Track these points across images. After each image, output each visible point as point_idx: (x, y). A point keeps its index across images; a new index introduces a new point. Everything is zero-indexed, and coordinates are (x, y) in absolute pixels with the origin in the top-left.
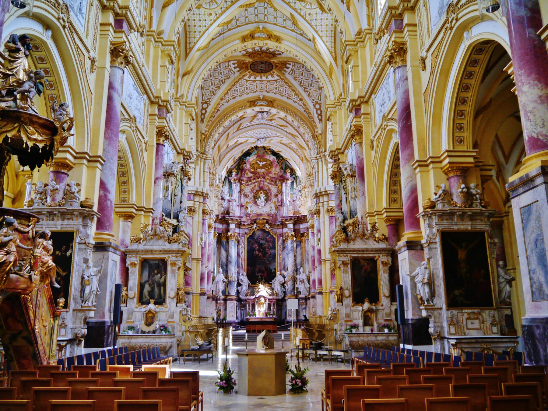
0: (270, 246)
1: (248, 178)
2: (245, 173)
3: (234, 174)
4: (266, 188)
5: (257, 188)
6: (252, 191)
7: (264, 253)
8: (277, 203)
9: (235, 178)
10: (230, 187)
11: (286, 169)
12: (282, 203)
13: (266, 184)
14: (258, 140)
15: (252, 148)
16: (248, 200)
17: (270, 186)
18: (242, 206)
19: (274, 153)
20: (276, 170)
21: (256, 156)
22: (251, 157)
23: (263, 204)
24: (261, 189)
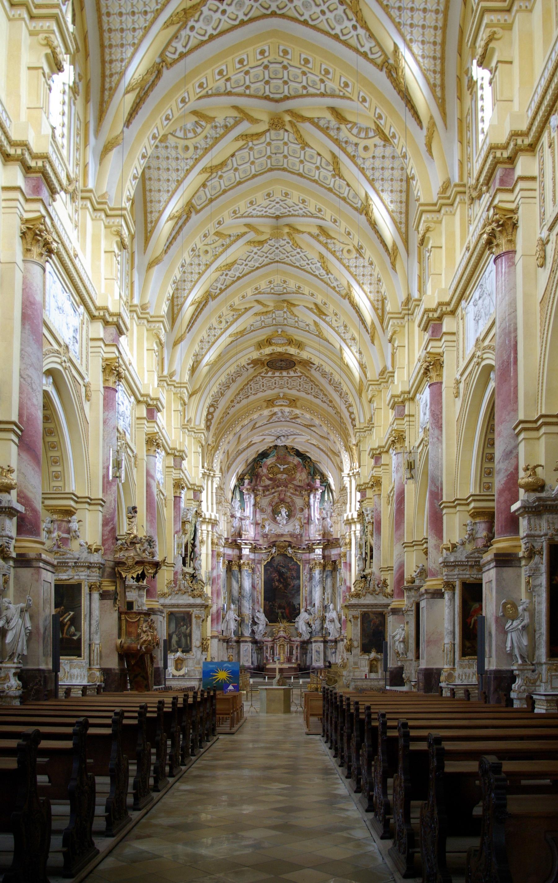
0: (293, 576)
1: (265, 486)
2: (260, 480)
3: (246, 481)
4: (289, 500)
5: (276, 500)
6: (270, 504)
7: (286, 585)
8: (302, 520)
9: (249, 487)
10: (242, 500)
11: (315, 474)
12: (309, 520)
13: (289, 494)
14: (279, 437)
15: (270, 448)
16: (265, 516)
17: (294, 497)
18: (257, 524)
19: (298, 454)
20: (301, 477)
21: (275, 458)
22: (268, 460)
23: (285, 522)
24: (282, 501)
